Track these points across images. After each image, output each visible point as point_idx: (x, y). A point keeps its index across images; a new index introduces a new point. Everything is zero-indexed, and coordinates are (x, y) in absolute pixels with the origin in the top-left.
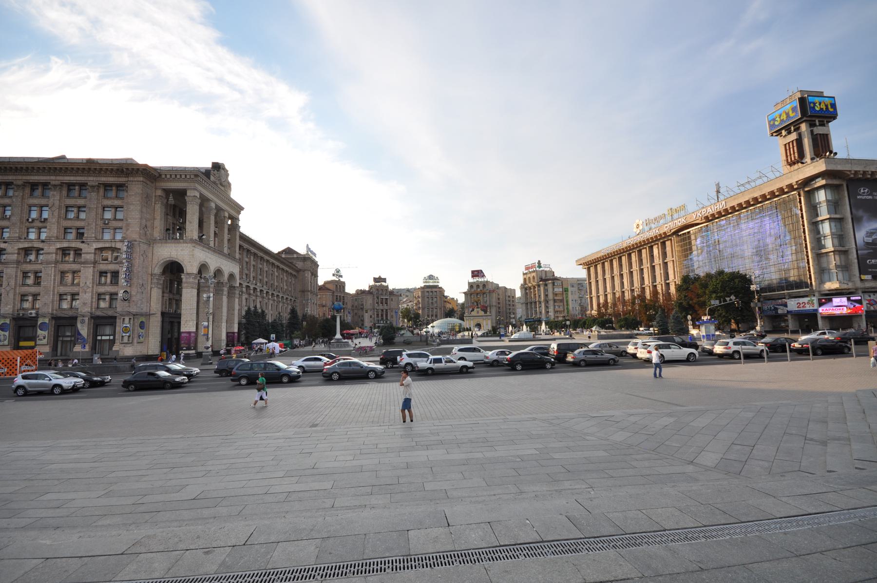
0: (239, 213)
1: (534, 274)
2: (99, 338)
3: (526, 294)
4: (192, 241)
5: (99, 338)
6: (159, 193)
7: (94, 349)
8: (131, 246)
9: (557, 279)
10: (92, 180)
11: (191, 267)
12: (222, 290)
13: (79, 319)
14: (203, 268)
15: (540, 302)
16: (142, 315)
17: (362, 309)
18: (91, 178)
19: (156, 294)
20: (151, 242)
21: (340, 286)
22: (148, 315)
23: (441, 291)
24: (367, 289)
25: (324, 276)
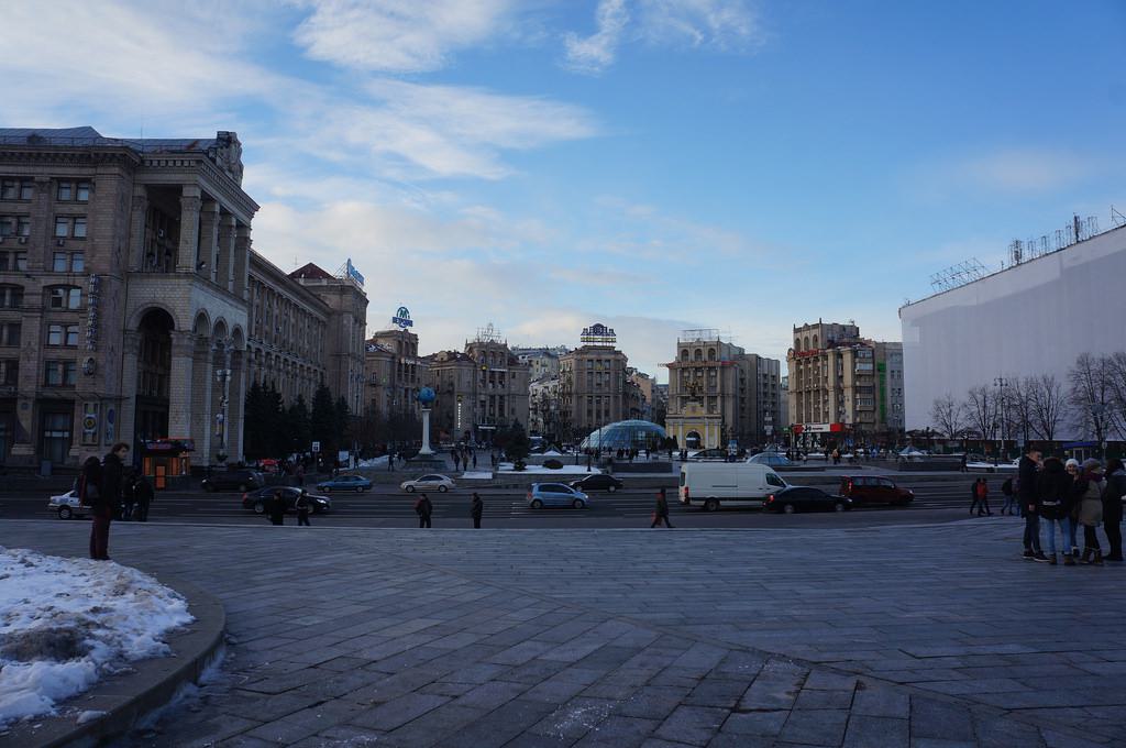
0: (251, 216)
1: (816, 332)
2: (48, 434)
3: (799, 372)
4: (188, 275)
5: (48, 434)
6: (140, 191)
7: (39, 450)
9: (864, 344)
10: (43, 172)
11: (185, 321)
13: (20, 403)
14: (202, 317)
15: (826, 392)
17: (451, 393)
18: (39, 170)
19: (131, 364)
20: (126, 276)
21: (408, 343)
22: (119, 400)
23: (620, 359)
24: (462, 351)
25: (378, 321)
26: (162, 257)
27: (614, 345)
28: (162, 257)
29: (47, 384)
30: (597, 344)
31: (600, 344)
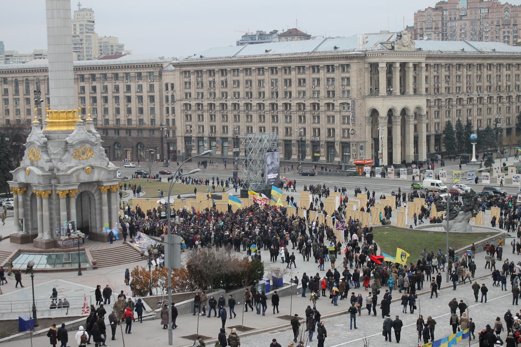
4: (382, 97)
6: (367, 66)
7: (343, 159)
8: (353, 102)
11: (383, 113)
12: (409, 121)
13: (336, 143)
14: (391, 112)
16: (362, 142)
18: (335, 62)
19: (368, 128)
20: (364, 98)
26: (374, 92)
28: (374, 92)
29: (344, 137)
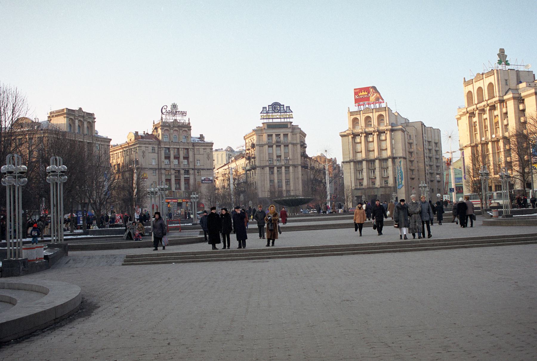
27: (291, 120)
30: (275, 121)
31: (279, 120)
